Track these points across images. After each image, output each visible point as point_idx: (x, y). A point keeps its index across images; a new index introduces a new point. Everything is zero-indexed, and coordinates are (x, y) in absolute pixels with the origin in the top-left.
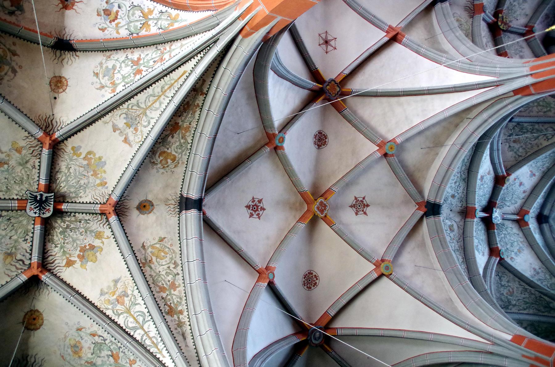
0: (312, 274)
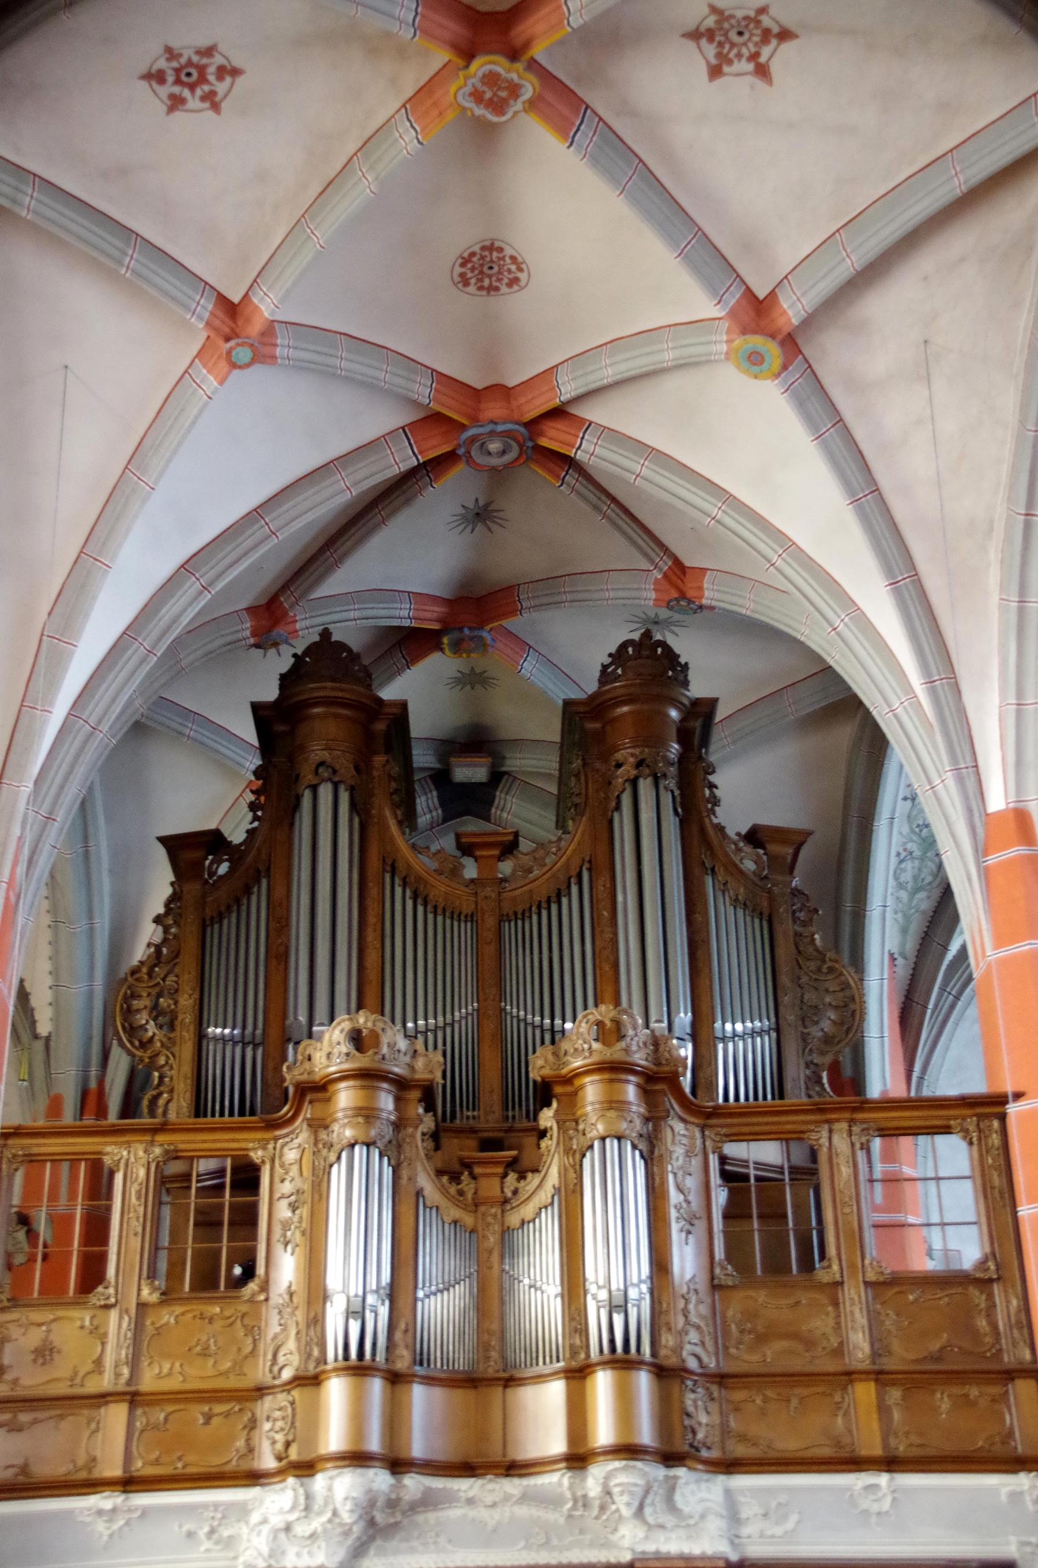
0: (500, 250)
